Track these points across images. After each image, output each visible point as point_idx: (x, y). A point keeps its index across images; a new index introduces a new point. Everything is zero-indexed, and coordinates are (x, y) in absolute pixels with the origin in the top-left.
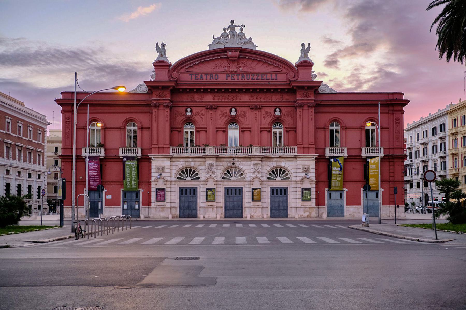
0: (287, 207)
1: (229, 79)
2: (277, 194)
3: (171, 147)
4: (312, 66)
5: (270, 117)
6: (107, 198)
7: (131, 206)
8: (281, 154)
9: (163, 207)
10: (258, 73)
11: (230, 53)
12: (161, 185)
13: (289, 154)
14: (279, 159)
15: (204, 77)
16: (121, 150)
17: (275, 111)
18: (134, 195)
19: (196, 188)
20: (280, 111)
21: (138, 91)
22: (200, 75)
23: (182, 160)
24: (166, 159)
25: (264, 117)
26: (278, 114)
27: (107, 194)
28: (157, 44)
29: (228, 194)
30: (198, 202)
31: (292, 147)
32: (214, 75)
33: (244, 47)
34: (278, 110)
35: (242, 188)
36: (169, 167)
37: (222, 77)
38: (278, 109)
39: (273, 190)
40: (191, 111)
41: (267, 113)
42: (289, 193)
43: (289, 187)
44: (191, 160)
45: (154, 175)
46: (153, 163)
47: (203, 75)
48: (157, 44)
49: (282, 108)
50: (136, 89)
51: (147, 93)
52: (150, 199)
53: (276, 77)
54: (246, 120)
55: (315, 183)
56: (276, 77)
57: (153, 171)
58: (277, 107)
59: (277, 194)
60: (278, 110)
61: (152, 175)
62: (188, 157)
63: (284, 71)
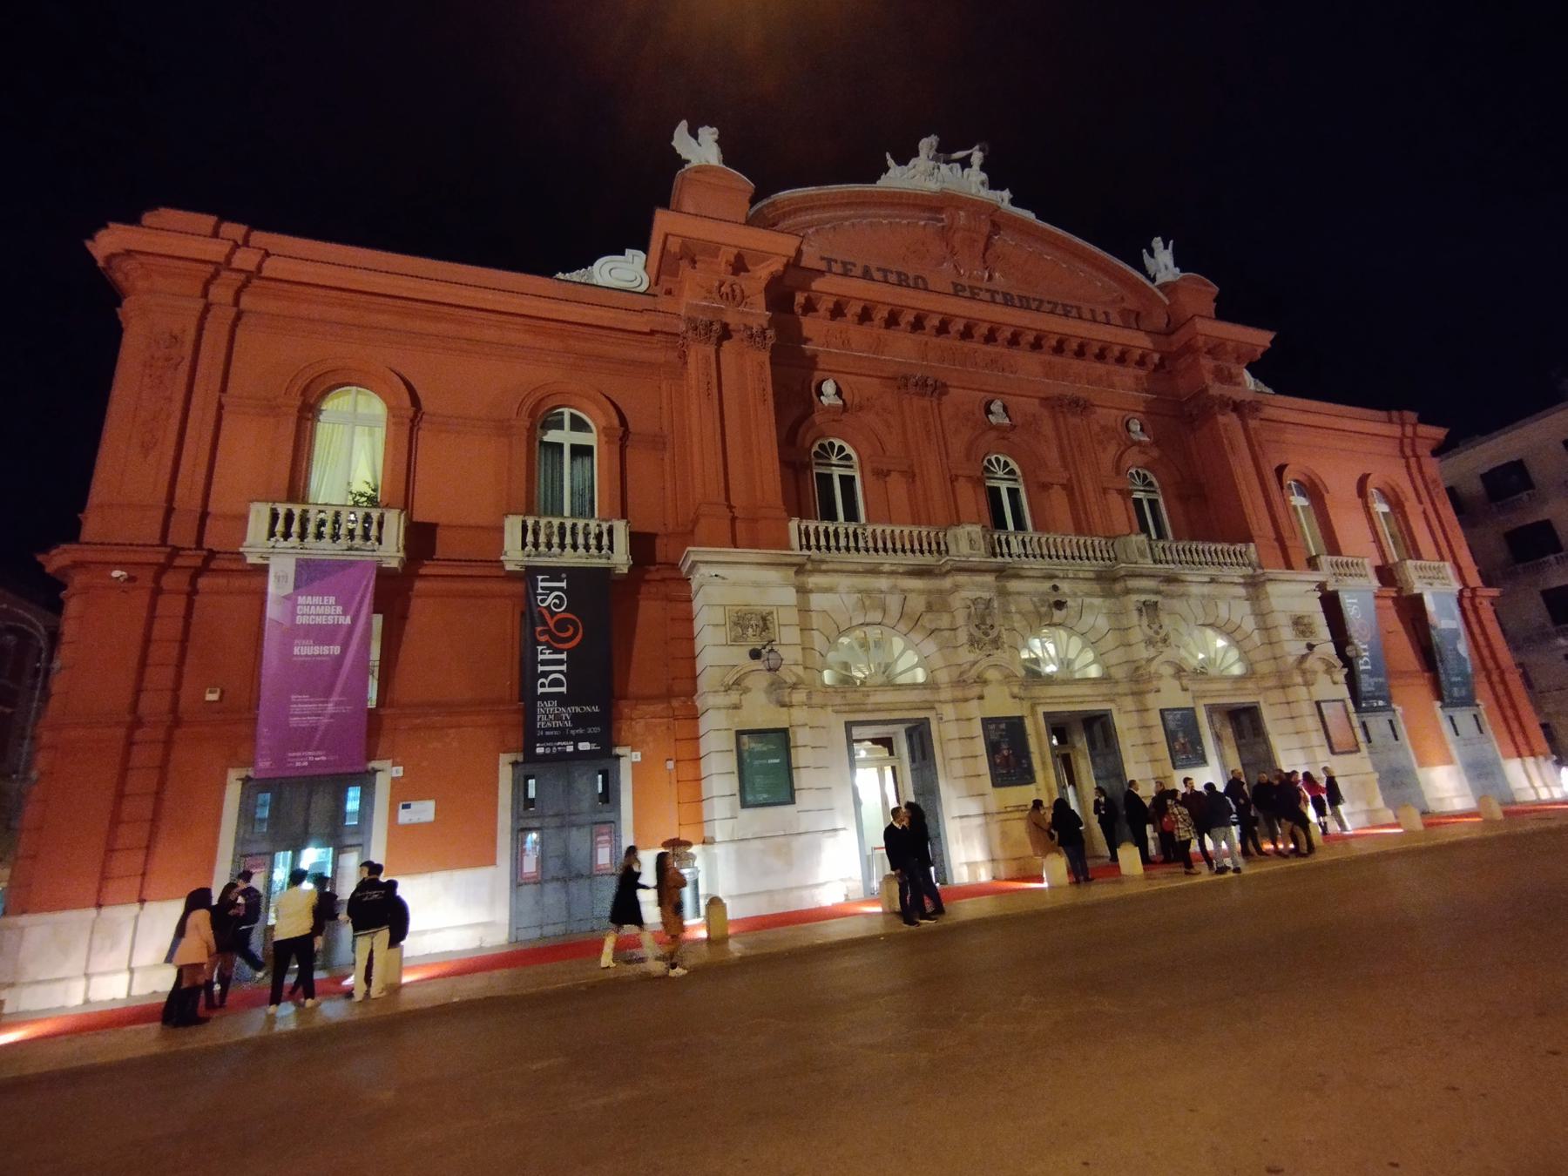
3: (793, 525)
6: (404, 817)
7: (566, 860)
12: (760, 712)
14: (1206, 589)
16: (512, 526)
19: (925, 722)
23: (844, 582)
24: (772, 575)
25: (1100, 442)
27: (403, 795)
31: (1238, 547)
36: (793, 616)
40: (839, 392)
44: (883, 583)
62: (874, 571)
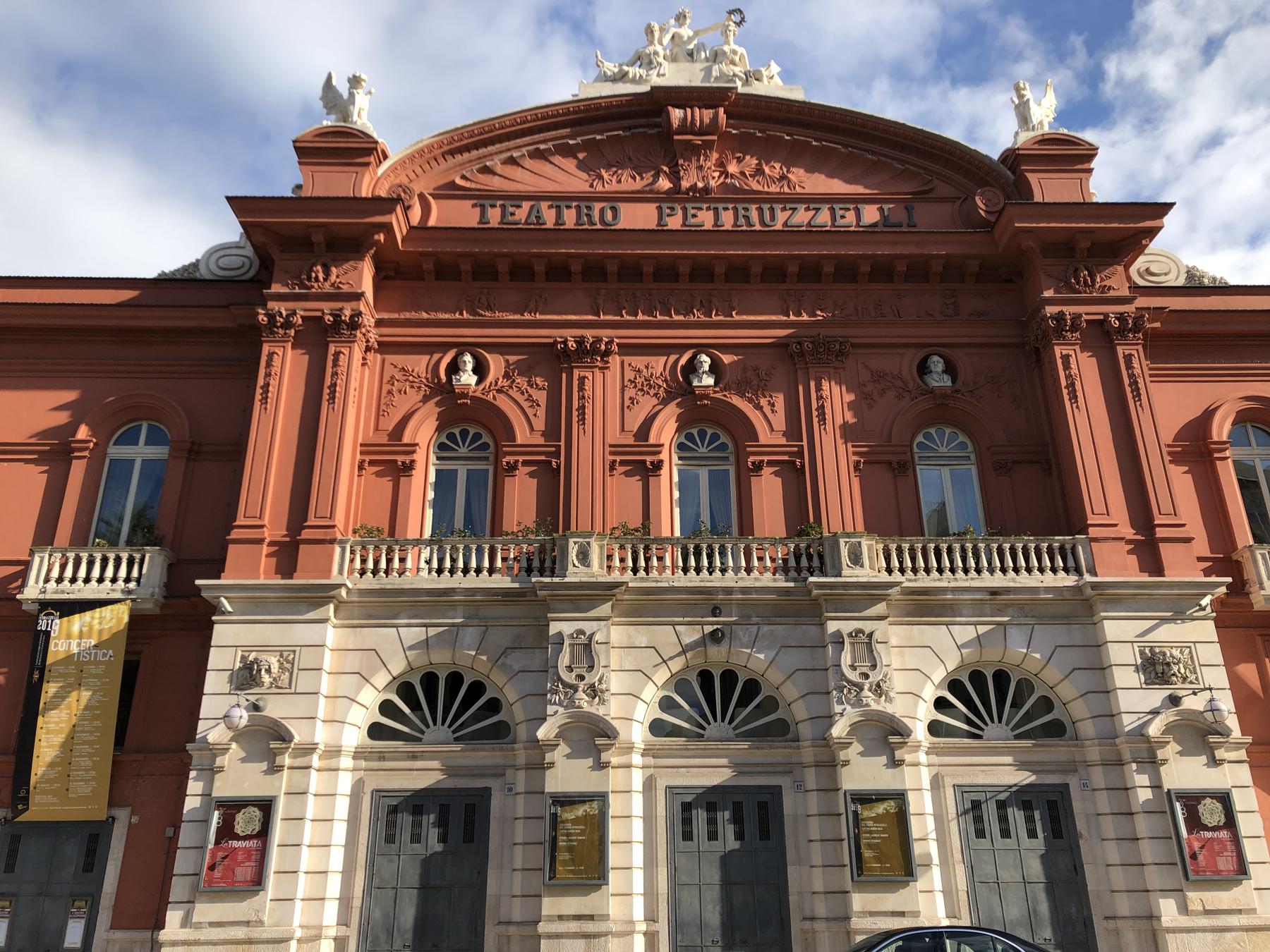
0: (1088, 924)
1: (674, 223)
2: (1005, 833)
4: (1094, 156)
5: (899, 397)
8: (998, 580)
9: (240, 933)
10: (813, 201)
11: (676, 114)
13: (1049, 580)
15: (549, 217)
17: (923, 369)
18: (73, 851)
19: (485, 793)
20: (950, 369)
21: (204, 273)
22: (526, 205)
26: (938, 379)
28: (329, 78)
29: (687, 836)
30: (491, 889)
32: (597, 206)
33: (741, 89)
34: (937, 364)
35: (776, 792)
37: (639, 217)
38: (936, 358)
39: (976, 805)
41: (878, 376)
42: (1080, 825)
43: (1074, 783)
45: (219, 709)
46: (221, 633)
47: (544, 205)
48: (329, 78)
49: (960, 357)
50: (195, 265)
51: (251, 281)
52: (168, 874)
53: (910, 217)
54: (767, 409)
55: (1242, 754)
56: (910, 217)
57: (214, 682)
58: (935, 348)
59: (1005, 833)
60: (937, 364)
61: (210, 706)
63: (943, 189)
